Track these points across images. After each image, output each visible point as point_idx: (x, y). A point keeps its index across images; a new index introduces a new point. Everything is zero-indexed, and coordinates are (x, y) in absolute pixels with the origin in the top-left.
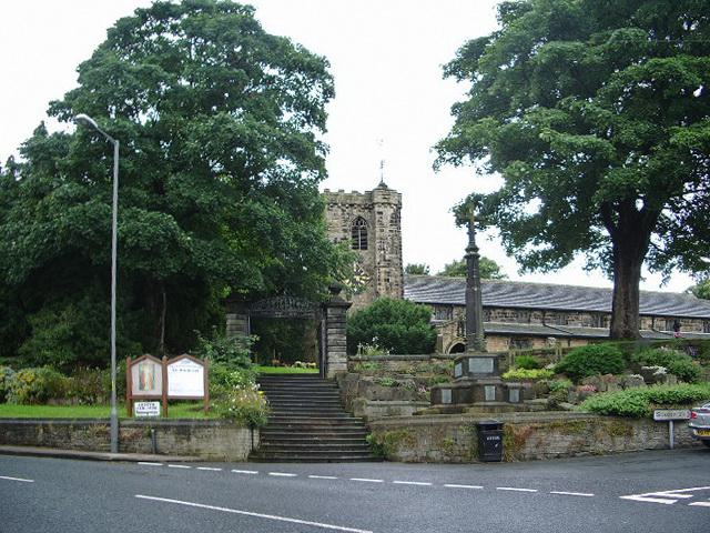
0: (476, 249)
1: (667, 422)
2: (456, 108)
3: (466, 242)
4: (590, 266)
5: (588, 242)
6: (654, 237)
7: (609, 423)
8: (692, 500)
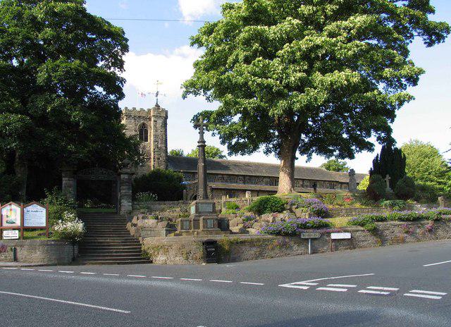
0: (204, 142)
1: (307, 239)
2: (196, 64)
3: (198, 137)
4: (268, 152)
5: (267, 139)
6: (303, 136)
7: (281, 238)
8: (318, 286)
